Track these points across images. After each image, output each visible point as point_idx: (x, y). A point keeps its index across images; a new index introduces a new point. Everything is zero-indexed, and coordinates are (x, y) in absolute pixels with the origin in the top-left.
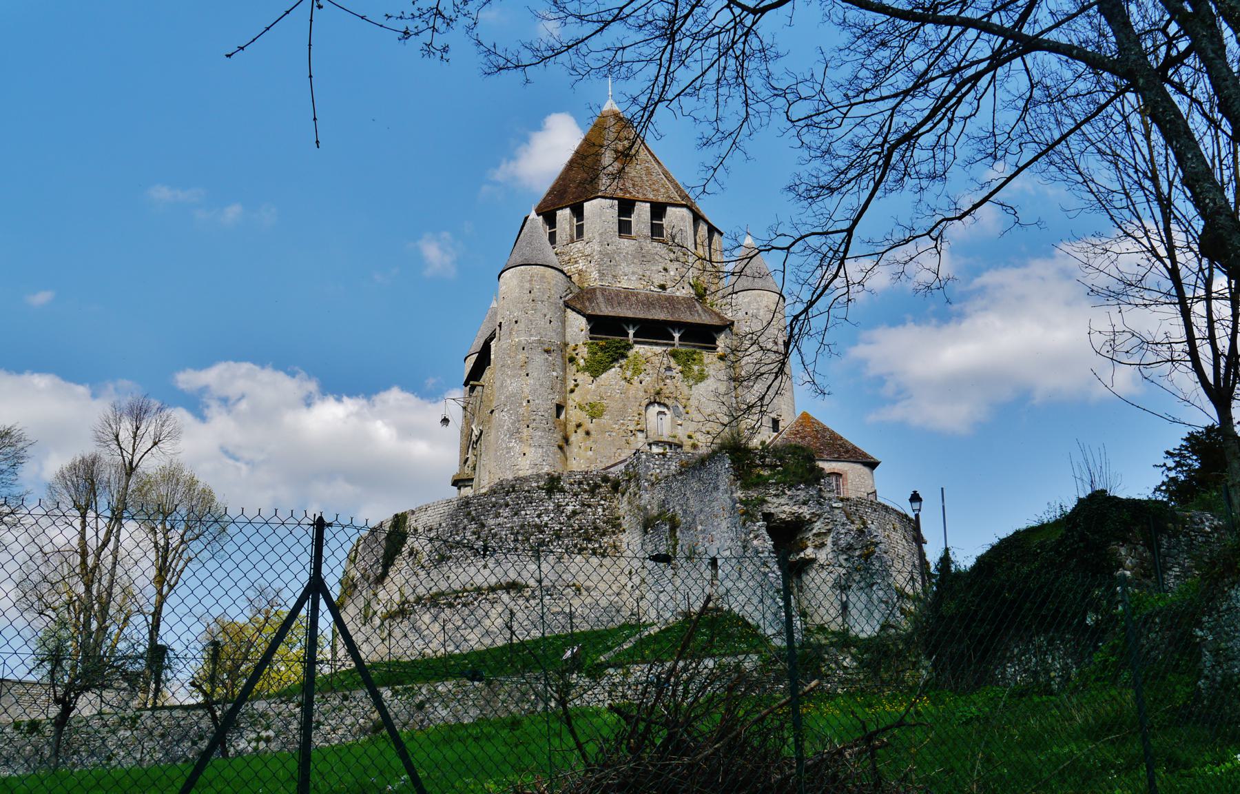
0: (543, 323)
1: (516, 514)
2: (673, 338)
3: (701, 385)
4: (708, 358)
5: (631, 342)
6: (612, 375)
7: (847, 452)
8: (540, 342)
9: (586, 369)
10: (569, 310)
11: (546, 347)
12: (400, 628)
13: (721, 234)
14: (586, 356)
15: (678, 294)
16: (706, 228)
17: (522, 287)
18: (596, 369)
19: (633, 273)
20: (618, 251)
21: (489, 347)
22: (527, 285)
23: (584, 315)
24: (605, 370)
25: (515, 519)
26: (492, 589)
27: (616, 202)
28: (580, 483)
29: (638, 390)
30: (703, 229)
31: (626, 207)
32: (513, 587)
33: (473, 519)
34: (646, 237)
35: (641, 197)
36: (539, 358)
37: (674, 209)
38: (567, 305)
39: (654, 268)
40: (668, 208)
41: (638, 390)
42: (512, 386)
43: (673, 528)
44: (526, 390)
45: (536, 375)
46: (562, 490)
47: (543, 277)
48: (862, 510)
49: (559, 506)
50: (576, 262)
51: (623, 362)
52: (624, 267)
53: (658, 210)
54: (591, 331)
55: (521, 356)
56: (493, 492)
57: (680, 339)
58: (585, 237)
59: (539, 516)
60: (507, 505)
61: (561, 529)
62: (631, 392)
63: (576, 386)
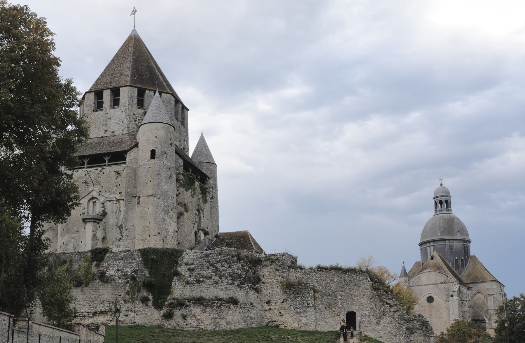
60: (226, 261)
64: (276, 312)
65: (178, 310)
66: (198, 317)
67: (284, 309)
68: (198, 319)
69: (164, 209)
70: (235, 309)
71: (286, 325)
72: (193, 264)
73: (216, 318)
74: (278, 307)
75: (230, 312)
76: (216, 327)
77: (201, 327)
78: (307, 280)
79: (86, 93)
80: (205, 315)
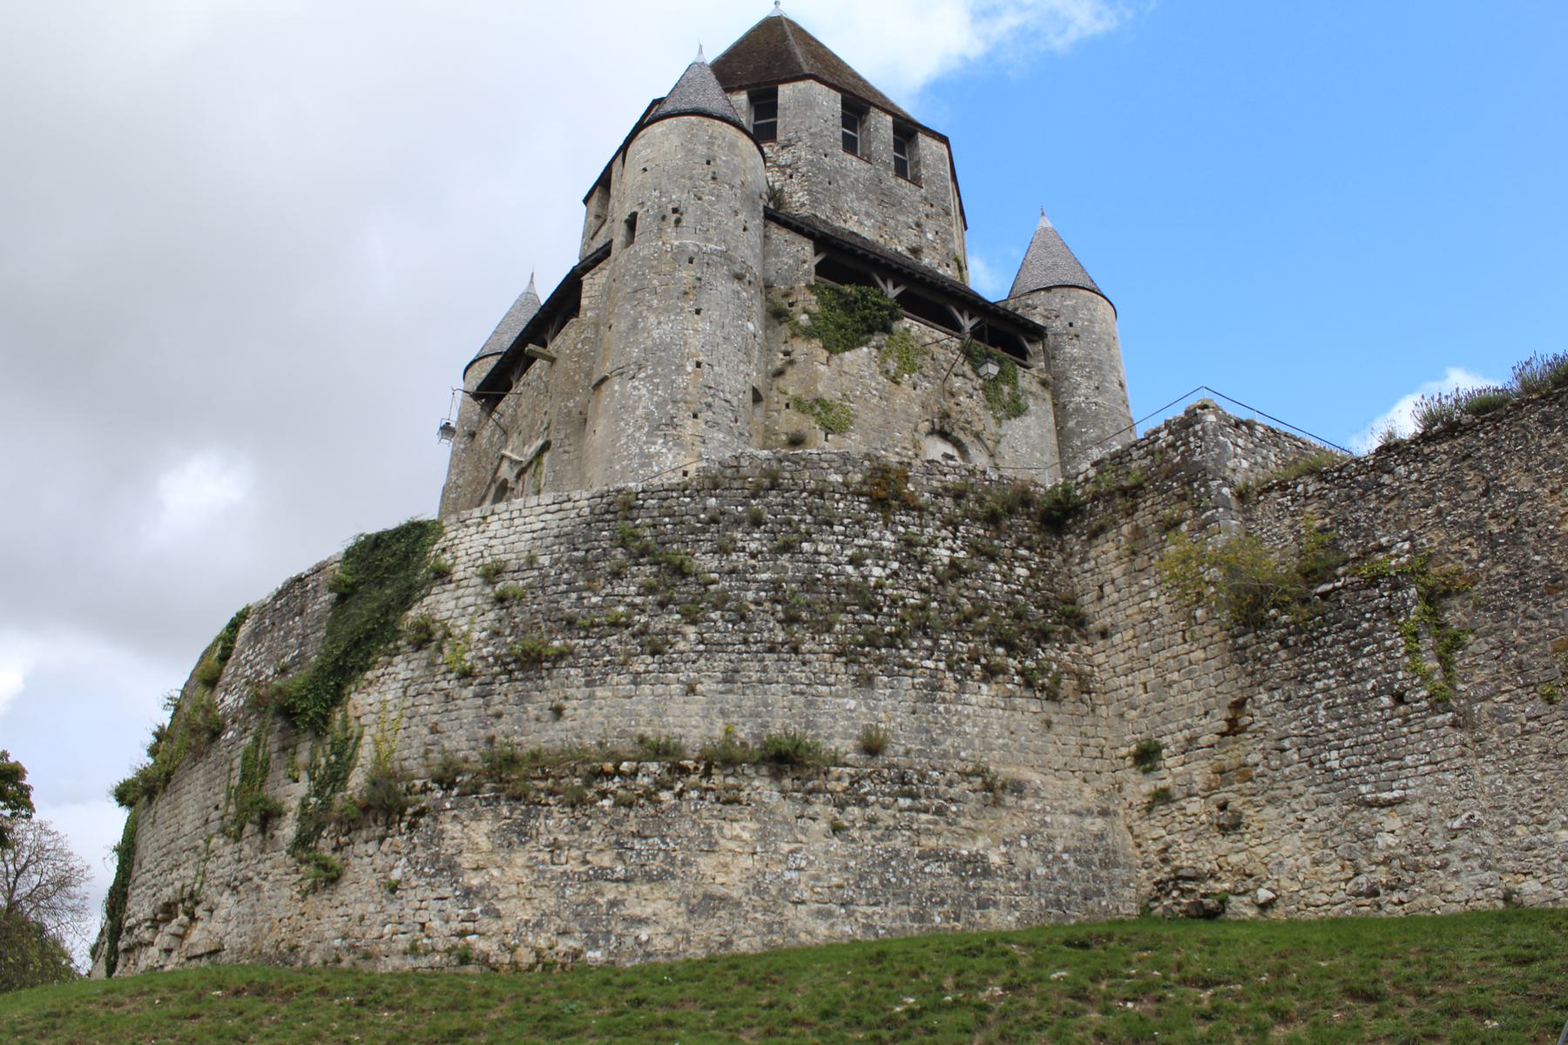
1: (787, 548)
3: (1015, 422)
9: (809, 334)
10: (773, 226)
11: (737, 269)
12: (369, 859)
14: (815, 309)
15: (940, 271)
17: (690, 152)
18: (840, 339)
19: (867, 214)
20: (841, 171)
21: (581, 283)
22: (702, 150)
23: (810, 235)
24: (849, 347)
25: (784, 559)
26: (721, 759)
28: (958, 495)
29: (910, 400)
32: (786, 760)
33: (644, 552)
36: (723, 288)
37: (929, 140)
39: (901, 218)
41: (910, 400)
42: (659, 328)
43: (1433, 598)
44: (695, 342)
45: (716, 315)
46: (909, 505)
47: (732, 146)
49: (910, 544)
54: (820, 269)
55: (686, 275)
56: (713, 484)
58: (780, 137)
59: (855, 561)
60: (757, 522)
61: (923, 607)
62: (899, 401)
63: (791, 363)
64: (1195, 806)
65: (372, 847)
66: (475, 881)
67: (1244, 772)
68: (468, 892)
69: (648, 416)
70: (787, 809)
71: (1264, 894)
72: (531, 561)
73: (602, 874)
74: (1200, 772)
75: (742, 829)
76: (593, 943)
77: (479, 944)
78: (1369, 533)
79: (586, 201)
80: (520, 858)
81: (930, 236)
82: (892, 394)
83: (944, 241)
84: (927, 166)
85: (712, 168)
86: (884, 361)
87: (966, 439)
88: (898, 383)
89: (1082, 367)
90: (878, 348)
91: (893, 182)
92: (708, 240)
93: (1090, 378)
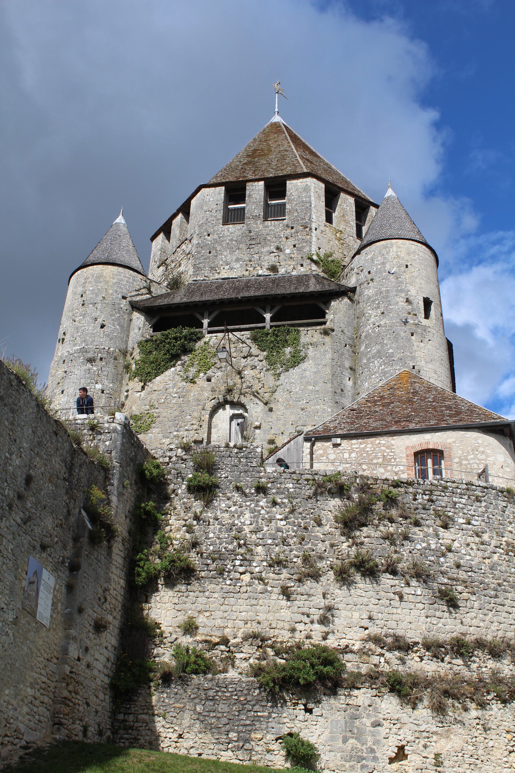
0: (93, 328)
2: (263, 320)
4: (309, 335)
5: (204, 332)
6: (169, 378)
7: (458, 413)
8: (84, 351)
11: (90, 355)
13: (377, 206)
16: (351, 200)
19: (237, 260)
27: (223, 188)
30: (346, 204)
31: (235, 192)
34: (255, 218)
35: (250, 177)
37: (294, 182)
38: (135, 306)
40: (288, 182)
48: (443, 501)
50: (180, 266)
51: (185, 358)
52: (226, 255)
53: (276, 188)
57: (272, 319)
81: (288, 251)
82: (189, 391)
83: (299, 250)
84: (290, 201)
85: (83, 298)
86: (186, 371)
87: (243, 400)
88: (194, 383)
89: (374, 301)
90: (183, 365)
91: (261, 227)
92: (75, 345)
93: (378, 307)
